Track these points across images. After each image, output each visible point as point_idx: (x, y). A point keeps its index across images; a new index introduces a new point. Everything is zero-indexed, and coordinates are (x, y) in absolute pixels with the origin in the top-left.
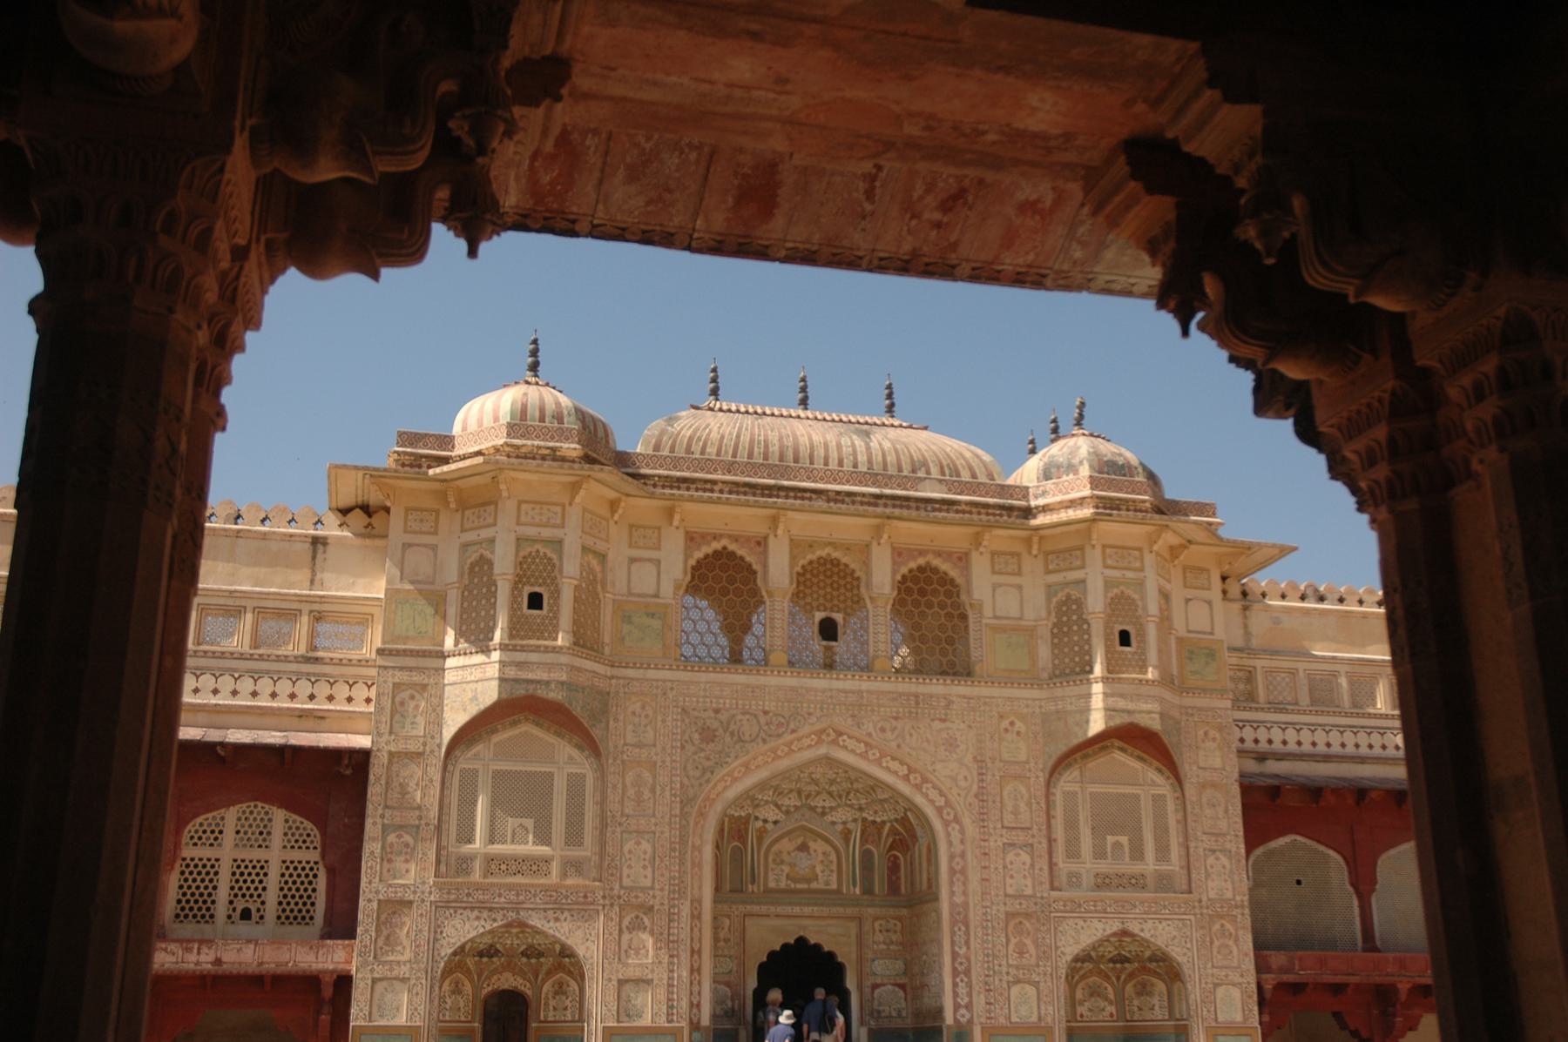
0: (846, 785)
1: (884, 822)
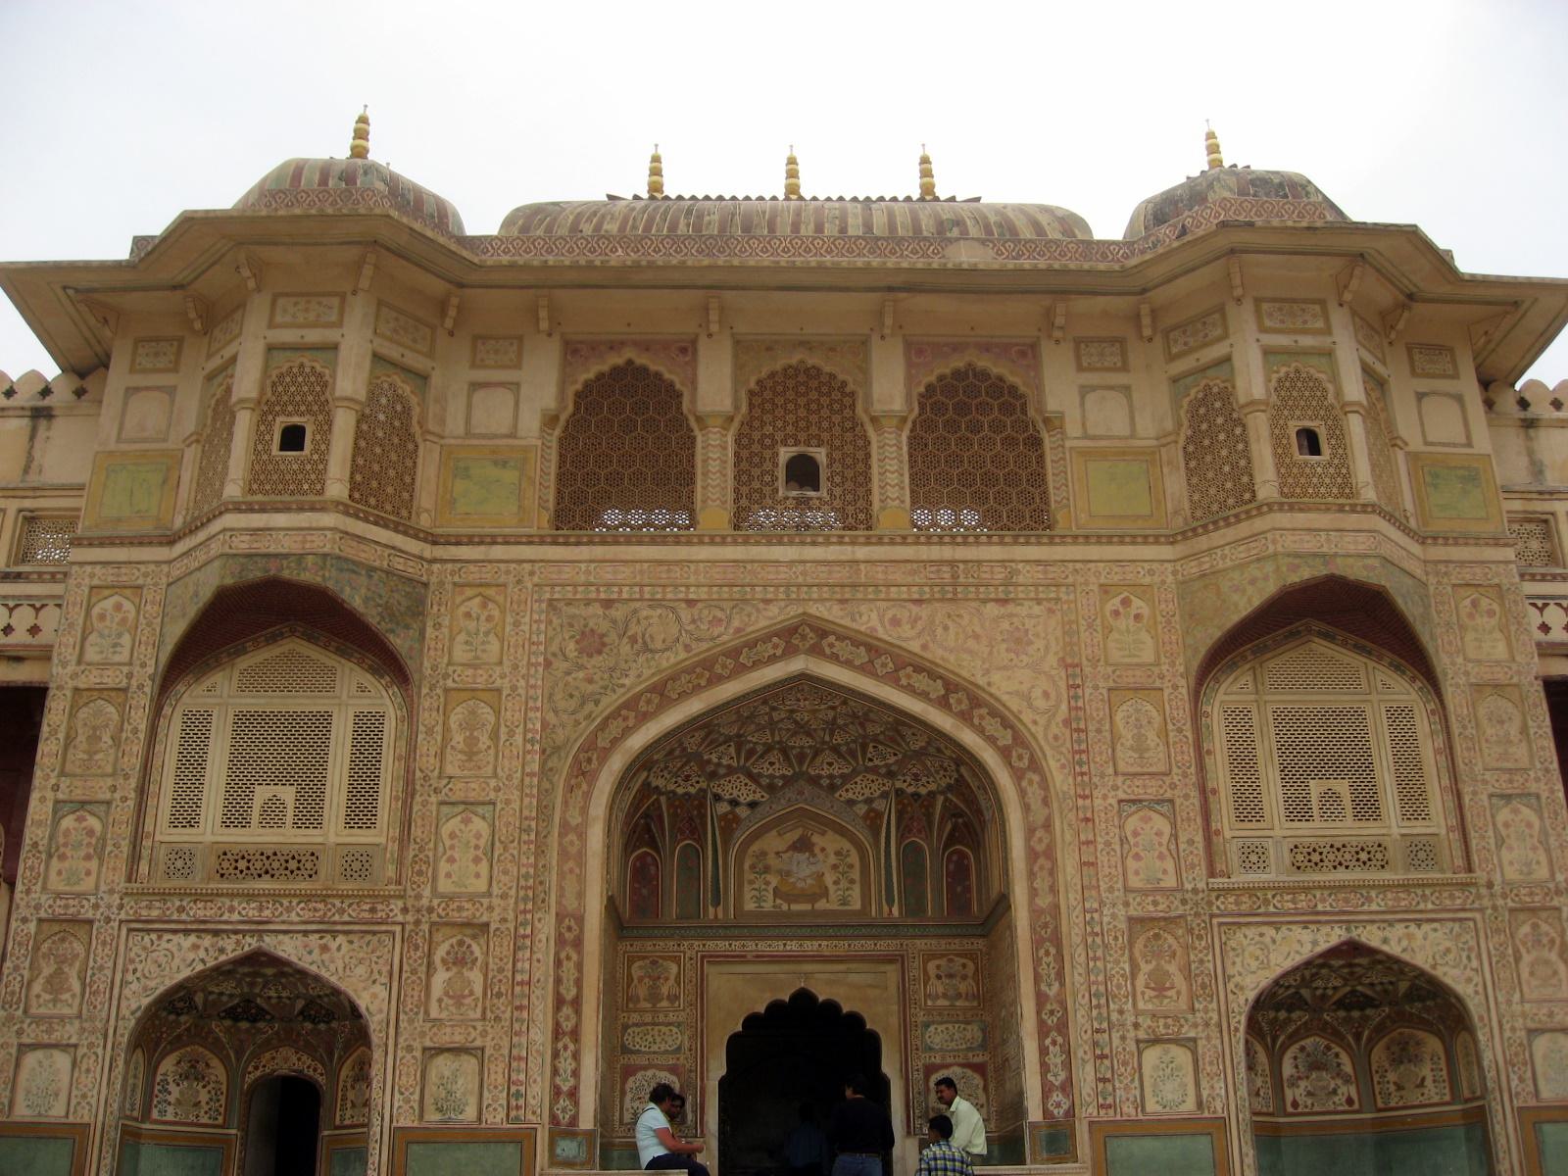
0: (855, 730)
1: (932, 794)
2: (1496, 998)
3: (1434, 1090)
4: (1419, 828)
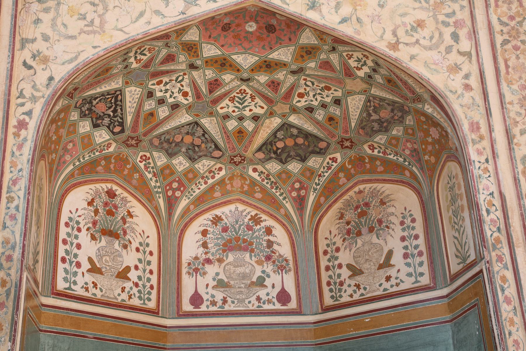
2: (501, 96)
3: (405, 270)
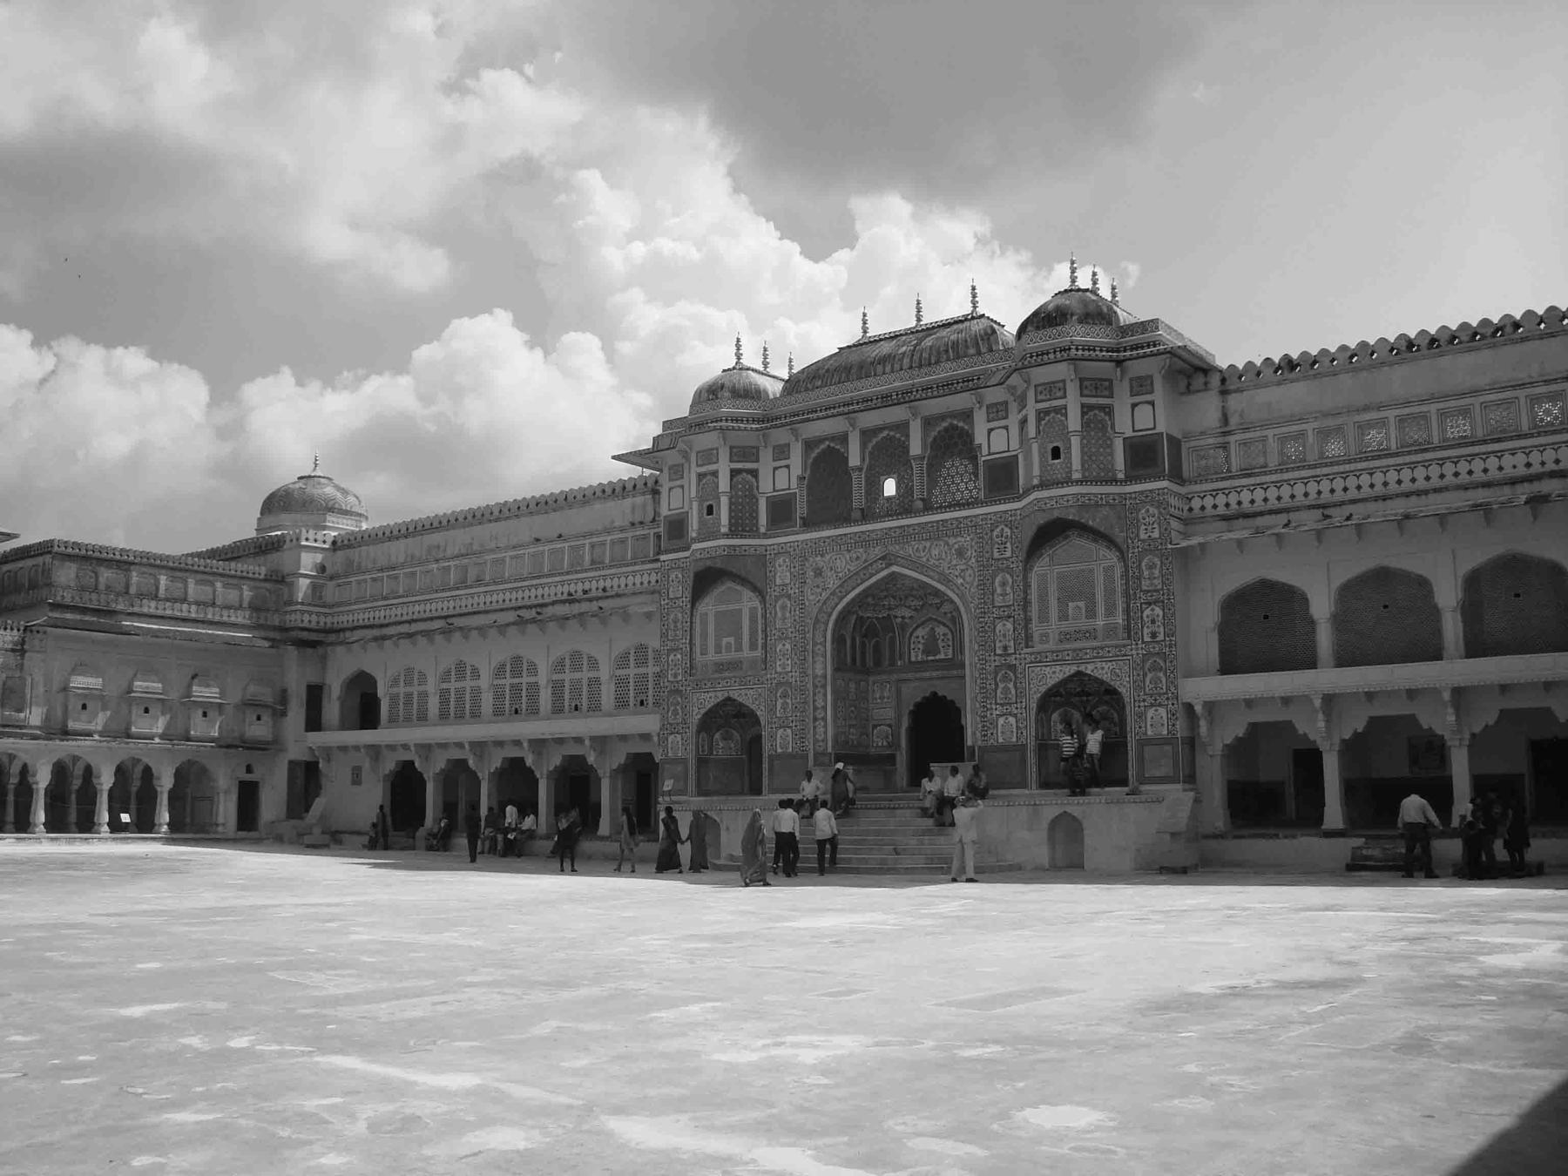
4: (1111, 620)
